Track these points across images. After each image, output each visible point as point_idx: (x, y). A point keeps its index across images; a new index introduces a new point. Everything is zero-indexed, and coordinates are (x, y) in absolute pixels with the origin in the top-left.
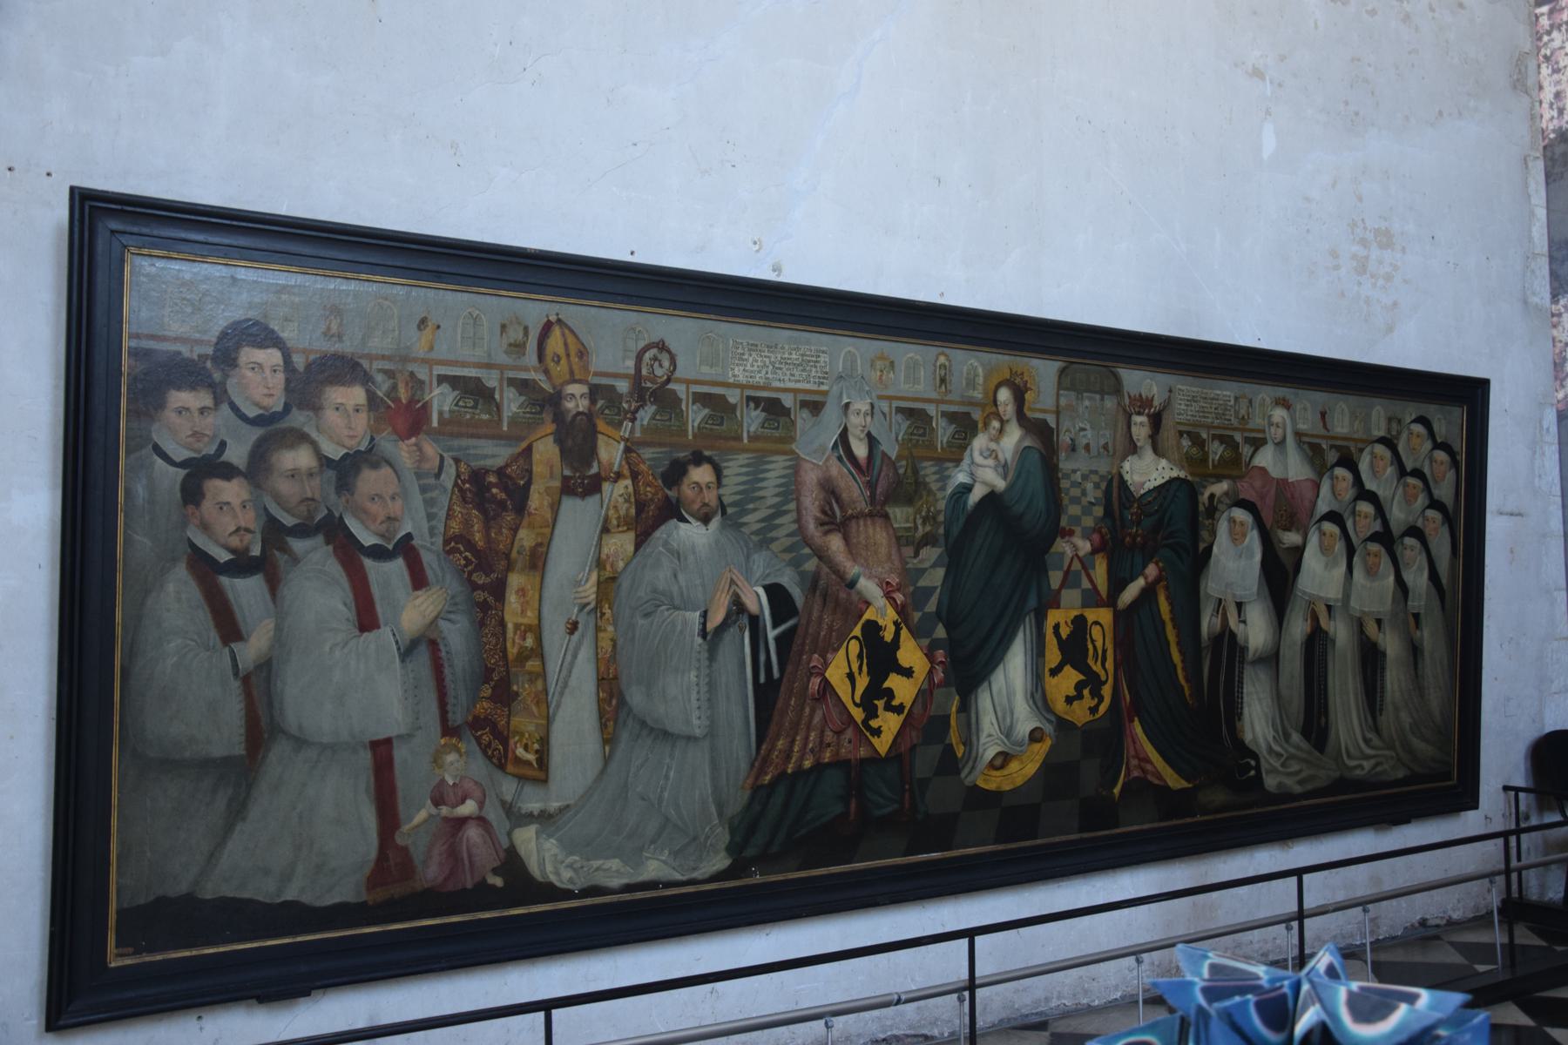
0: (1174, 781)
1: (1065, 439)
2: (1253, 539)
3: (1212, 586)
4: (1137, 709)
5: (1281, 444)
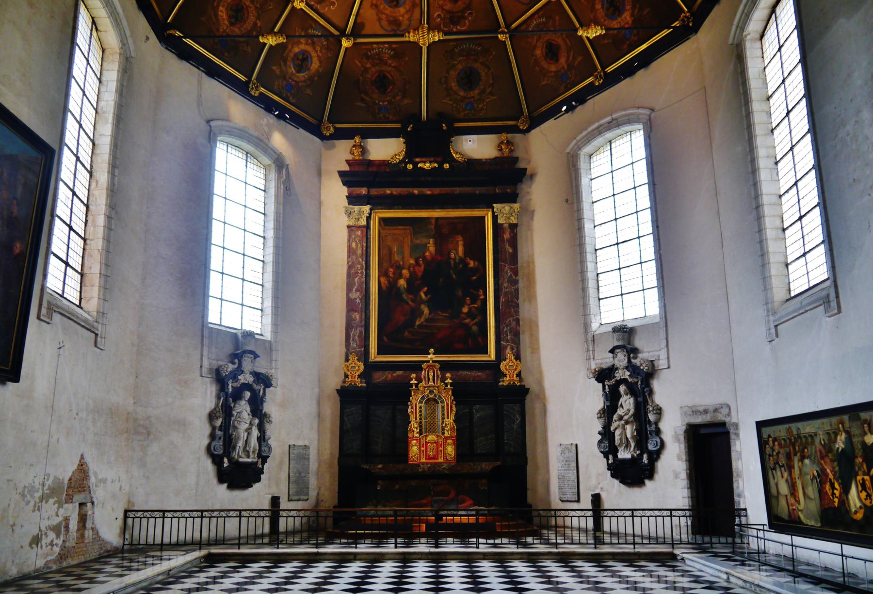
1: (852, 433)
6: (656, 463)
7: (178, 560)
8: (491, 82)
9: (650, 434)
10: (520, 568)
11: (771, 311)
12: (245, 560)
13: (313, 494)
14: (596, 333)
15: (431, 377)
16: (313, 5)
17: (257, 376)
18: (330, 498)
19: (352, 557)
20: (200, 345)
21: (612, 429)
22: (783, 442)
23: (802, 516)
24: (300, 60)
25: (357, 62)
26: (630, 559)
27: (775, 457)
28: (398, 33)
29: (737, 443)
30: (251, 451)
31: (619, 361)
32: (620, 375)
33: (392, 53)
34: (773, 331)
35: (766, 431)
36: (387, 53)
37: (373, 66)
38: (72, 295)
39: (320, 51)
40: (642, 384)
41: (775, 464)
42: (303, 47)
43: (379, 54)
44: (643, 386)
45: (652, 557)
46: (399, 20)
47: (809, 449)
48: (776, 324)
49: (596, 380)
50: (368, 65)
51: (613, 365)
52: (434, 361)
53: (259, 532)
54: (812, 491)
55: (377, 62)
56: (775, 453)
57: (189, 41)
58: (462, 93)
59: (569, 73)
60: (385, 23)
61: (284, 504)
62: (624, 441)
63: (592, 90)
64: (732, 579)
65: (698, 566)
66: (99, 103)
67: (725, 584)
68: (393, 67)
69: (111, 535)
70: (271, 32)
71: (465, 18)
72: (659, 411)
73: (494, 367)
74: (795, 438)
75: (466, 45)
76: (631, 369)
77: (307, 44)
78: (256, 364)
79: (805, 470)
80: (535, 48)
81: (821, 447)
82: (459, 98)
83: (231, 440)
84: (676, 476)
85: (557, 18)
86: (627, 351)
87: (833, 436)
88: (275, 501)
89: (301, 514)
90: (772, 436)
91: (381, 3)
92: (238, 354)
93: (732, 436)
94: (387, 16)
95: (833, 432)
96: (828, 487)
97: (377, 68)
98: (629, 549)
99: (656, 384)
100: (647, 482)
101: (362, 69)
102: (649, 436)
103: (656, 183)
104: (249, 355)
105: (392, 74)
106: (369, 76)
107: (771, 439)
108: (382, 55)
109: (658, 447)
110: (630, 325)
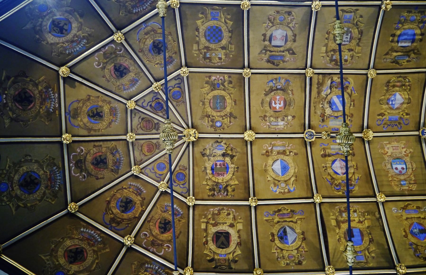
8: (29, 205)
16: (105, 49)
25: (42, 78)
33: (51, 110)
36: (51, 105)
37: (40, 92)
39: (62, 46)
43: (50, 99)
46: (78, 117)
55: (43, 96)
58: (16, 177)
60: (75, 105)
71: (81, 172)
75: (59, 176)
77: (75, 35)
80: (71, 238)
82: (12, 175)
85: (107, 250)
91: (91, 103)
94: (81, 108)
97: (38, 95)
105: (33, 110)
106: (31, 87)
108: (49, 101)
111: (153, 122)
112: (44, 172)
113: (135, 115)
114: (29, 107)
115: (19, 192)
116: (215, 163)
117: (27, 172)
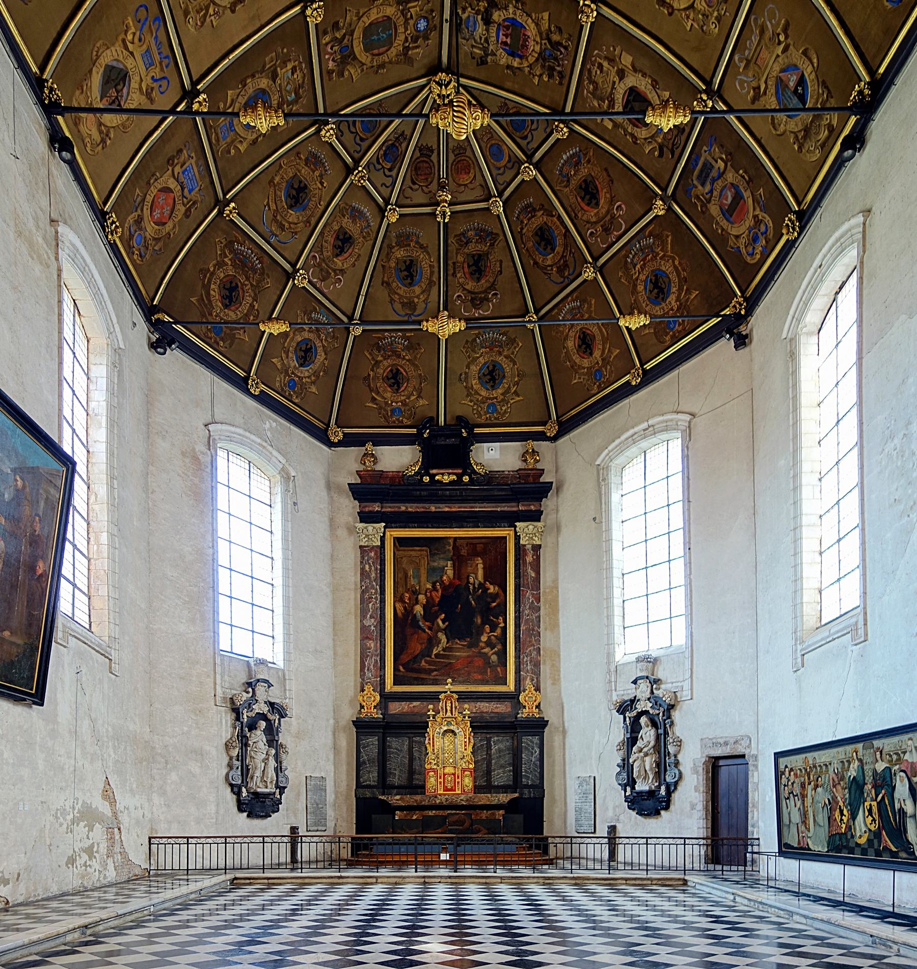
0: (894, 849)
2: (906, 780)
3: (897, 795)
4: (884, 828)
5: (911, 751)
6: (673, 795)
7: (207, 882)
9: (669, 766)
10: (538, 891)
11: (799, 640)
12: (271, 884)
13: (330, 824)
14: (620, 663)
15: (449, 708)
17: (272, 705)
18: (348, 829)
19: (374, 880)
20: (212, 673)
21: (631, 761)
22: (798, 771)
23: (810, 843)
24: (303, 351)
26: (642, 884)
27: (790, 787)
28: (413, 318)
29: (756, 774)
30: (269, 781)
31: (642, 692)
32: (640, 707)
34: (799, 660)
35: (783, 761)
38: (82, 617)
40: (664, 715)
41: (789, 793)
42: (306, 335)
44: (665, 718)
45: (664, 883)
47: (823, 777)
48: (803, 653)
49: (618, 711)
50: (380, 358)
51: (635, 697)
52: (451, 692)
53: (275, 861)
54: (822, 818)
56: (790, 783)
57: (179, 328)
59: (604, 369)
61: (302, 831)
62: (643, 772)
63: (627, 391)
64: (738, 899)
65: (708, 890)
66: (90, 403)
67: (732, 904)
68: (408, 360)
69: (139, 858)
70: (270, 319)
72: (679, 743)
73: (513, 698)
74: (810, 767)
76: (653, 701)
78: (270, 693)
79: (817, 798)
81: (834, 776)
83: (248, 770)
84: (693, 807)
86: (650, 682)
87: (846, 764)
88: (294, 830)
89: (324, 839)
90: (789, 766)
92: (251, 682)
93: (751, 768)
95: (847, 761)
96: (837, 814)
97: (389, 361)
98: (643, 875)
99: (676, 715)
100: (663, 812)
101: (373, 362)
102: (668, 768)
103: (691, 500)
104: (262, 684)
107: (787, 769)
109: (676, 779)
110: (654, 655)
111: (418, 160)
112: (481, 356)
113: (407, 198)
114: (404, 373)
115: (500, 391)
116: (501, 44)
117: (479, 378)
